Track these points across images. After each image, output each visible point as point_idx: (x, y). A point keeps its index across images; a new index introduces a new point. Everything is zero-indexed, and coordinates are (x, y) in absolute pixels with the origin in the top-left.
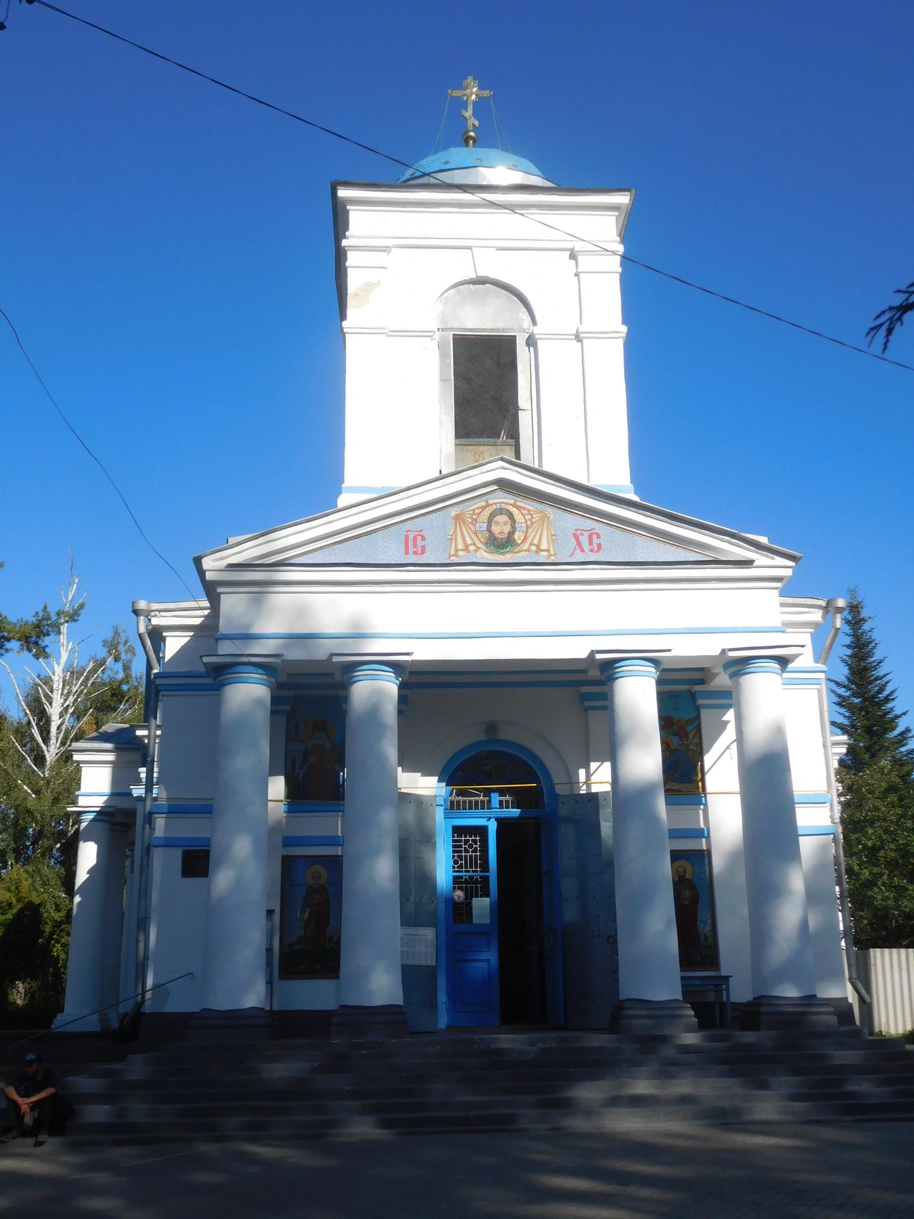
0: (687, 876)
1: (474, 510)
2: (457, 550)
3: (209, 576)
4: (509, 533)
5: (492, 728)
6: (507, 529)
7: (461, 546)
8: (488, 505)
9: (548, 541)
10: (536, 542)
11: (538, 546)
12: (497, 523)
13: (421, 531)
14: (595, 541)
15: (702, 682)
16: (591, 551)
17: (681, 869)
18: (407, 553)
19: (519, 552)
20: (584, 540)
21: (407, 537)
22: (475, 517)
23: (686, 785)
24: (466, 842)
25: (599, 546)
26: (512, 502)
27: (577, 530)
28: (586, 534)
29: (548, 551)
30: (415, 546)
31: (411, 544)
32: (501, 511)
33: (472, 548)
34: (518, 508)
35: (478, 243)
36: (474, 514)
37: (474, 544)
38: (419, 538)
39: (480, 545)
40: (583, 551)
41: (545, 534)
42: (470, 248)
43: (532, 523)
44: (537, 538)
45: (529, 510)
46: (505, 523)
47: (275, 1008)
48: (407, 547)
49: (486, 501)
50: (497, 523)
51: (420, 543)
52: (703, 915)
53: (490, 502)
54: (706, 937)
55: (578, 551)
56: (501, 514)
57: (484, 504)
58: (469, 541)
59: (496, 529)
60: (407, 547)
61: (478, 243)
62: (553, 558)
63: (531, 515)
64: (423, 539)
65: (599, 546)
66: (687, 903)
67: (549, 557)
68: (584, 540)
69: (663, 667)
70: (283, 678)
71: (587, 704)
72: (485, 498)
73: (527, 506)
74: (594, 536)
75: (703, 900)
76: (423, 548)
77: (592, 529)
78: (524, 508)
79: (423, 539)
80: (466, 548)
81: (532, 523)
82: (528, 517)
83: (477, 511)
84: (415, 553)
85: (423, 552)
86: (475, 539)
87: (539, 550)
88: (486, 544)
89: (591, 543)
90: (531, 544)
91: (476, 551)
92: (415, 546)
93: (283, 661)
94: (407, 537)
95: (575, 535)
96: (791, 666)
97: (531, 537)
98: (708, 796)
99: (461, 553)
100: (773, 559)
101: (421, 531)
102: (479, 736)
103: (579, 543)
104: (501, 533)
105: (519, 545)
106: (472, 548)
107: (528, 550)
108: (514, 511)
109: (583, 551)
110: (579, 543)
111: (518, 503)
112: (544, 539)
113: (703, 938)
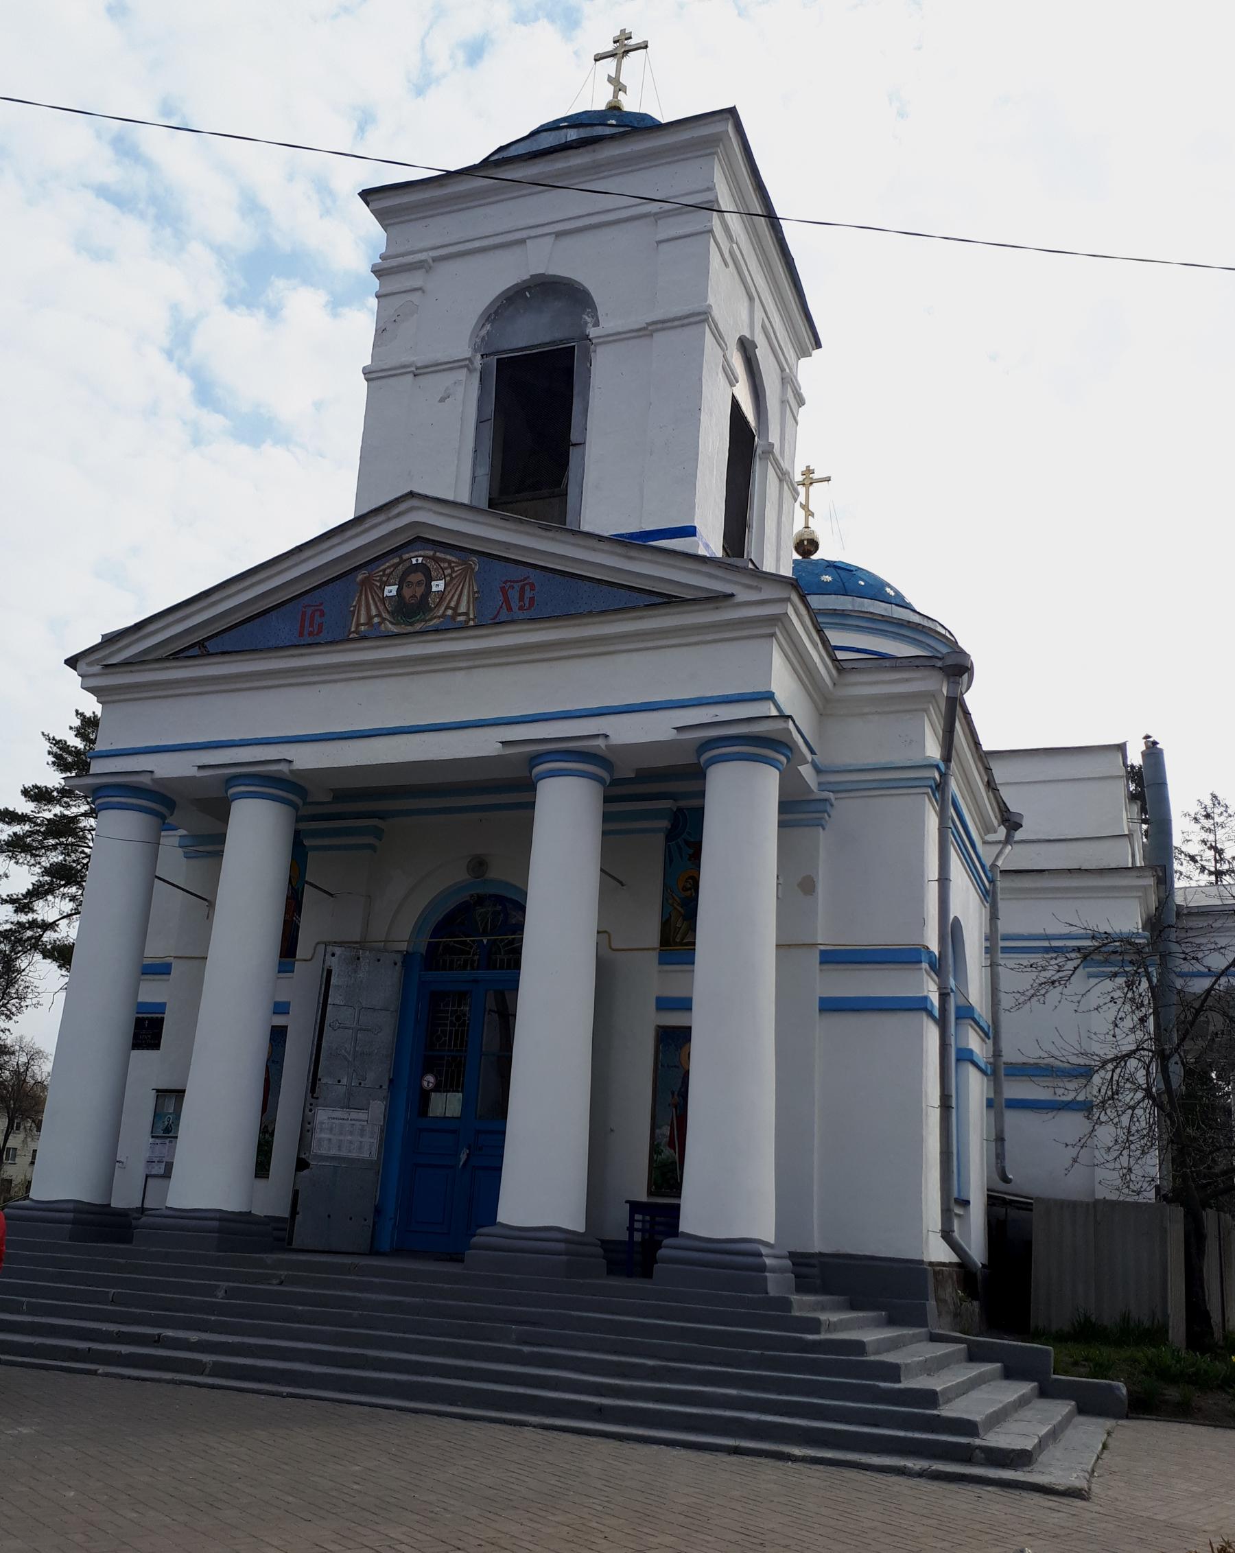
1: (384, 570)
2: (358, 625)
5: (479, 865)
6: (420, 591)
8: (402, 561)
9: (468, 602)
10: (453, 604)
11: (455, 609)
14: (528, 594)
16: (521, 608)
18: (301, 634)
19: (431, 620)
20: (514, 595)
21: (304, 614)
22: (384, 579)
25: (532, 600)
26: (431, 553)
27: (505, 582)
28: (517, 586)
29: (467, 614)
30: (311, 625)
31: (307, 624)
33: (376, 620)
34: (436, 560)
35: (533, 233)
37: (379, 615)
38: (318, 614)
39: (385, 615)
40: (510, 609)
41: (466, 591)
42: (522, 242)
43: (452, 579)
45: (450, 562)
46: (419, 583)
48: (302, 627)
49: (400, 557)
50: (410, 584)
51: (317, 619)
53: (406, 556)
55: (505, 610)
56: (415, 572)
57: (396, 560)
58: (374, 612)
59: (407, 592)
60: (302, 627)
61: (533, 233)
63: (452, 568)
65: (532, 600)
67: (467, 622)
68: (514, 595)
72: (399, 553)
73: (448, 557)
74: (527, 588)
76: (321, 625)
78: (444, 560)
79: (322, 614)
81: (452, 579)
83: (388, 571)
84: (310, 634)
85: (320, 631)
86: (381, 608)
87: (456, 613)
88: (391, 613)
89: (521, 599)
90: (448, 607)
92: (311, 625)
93: (155, 781)
94: (304, 614)
95: (503, 589)
99: (363, 628)
102: (458, 874)
103: (507, 600)
105: (431, 610)
107: (443, 616)
108: (431, 565)
109: (510, 609)
110: (507, 600)
111: (438, 554)
112: (465, 598)
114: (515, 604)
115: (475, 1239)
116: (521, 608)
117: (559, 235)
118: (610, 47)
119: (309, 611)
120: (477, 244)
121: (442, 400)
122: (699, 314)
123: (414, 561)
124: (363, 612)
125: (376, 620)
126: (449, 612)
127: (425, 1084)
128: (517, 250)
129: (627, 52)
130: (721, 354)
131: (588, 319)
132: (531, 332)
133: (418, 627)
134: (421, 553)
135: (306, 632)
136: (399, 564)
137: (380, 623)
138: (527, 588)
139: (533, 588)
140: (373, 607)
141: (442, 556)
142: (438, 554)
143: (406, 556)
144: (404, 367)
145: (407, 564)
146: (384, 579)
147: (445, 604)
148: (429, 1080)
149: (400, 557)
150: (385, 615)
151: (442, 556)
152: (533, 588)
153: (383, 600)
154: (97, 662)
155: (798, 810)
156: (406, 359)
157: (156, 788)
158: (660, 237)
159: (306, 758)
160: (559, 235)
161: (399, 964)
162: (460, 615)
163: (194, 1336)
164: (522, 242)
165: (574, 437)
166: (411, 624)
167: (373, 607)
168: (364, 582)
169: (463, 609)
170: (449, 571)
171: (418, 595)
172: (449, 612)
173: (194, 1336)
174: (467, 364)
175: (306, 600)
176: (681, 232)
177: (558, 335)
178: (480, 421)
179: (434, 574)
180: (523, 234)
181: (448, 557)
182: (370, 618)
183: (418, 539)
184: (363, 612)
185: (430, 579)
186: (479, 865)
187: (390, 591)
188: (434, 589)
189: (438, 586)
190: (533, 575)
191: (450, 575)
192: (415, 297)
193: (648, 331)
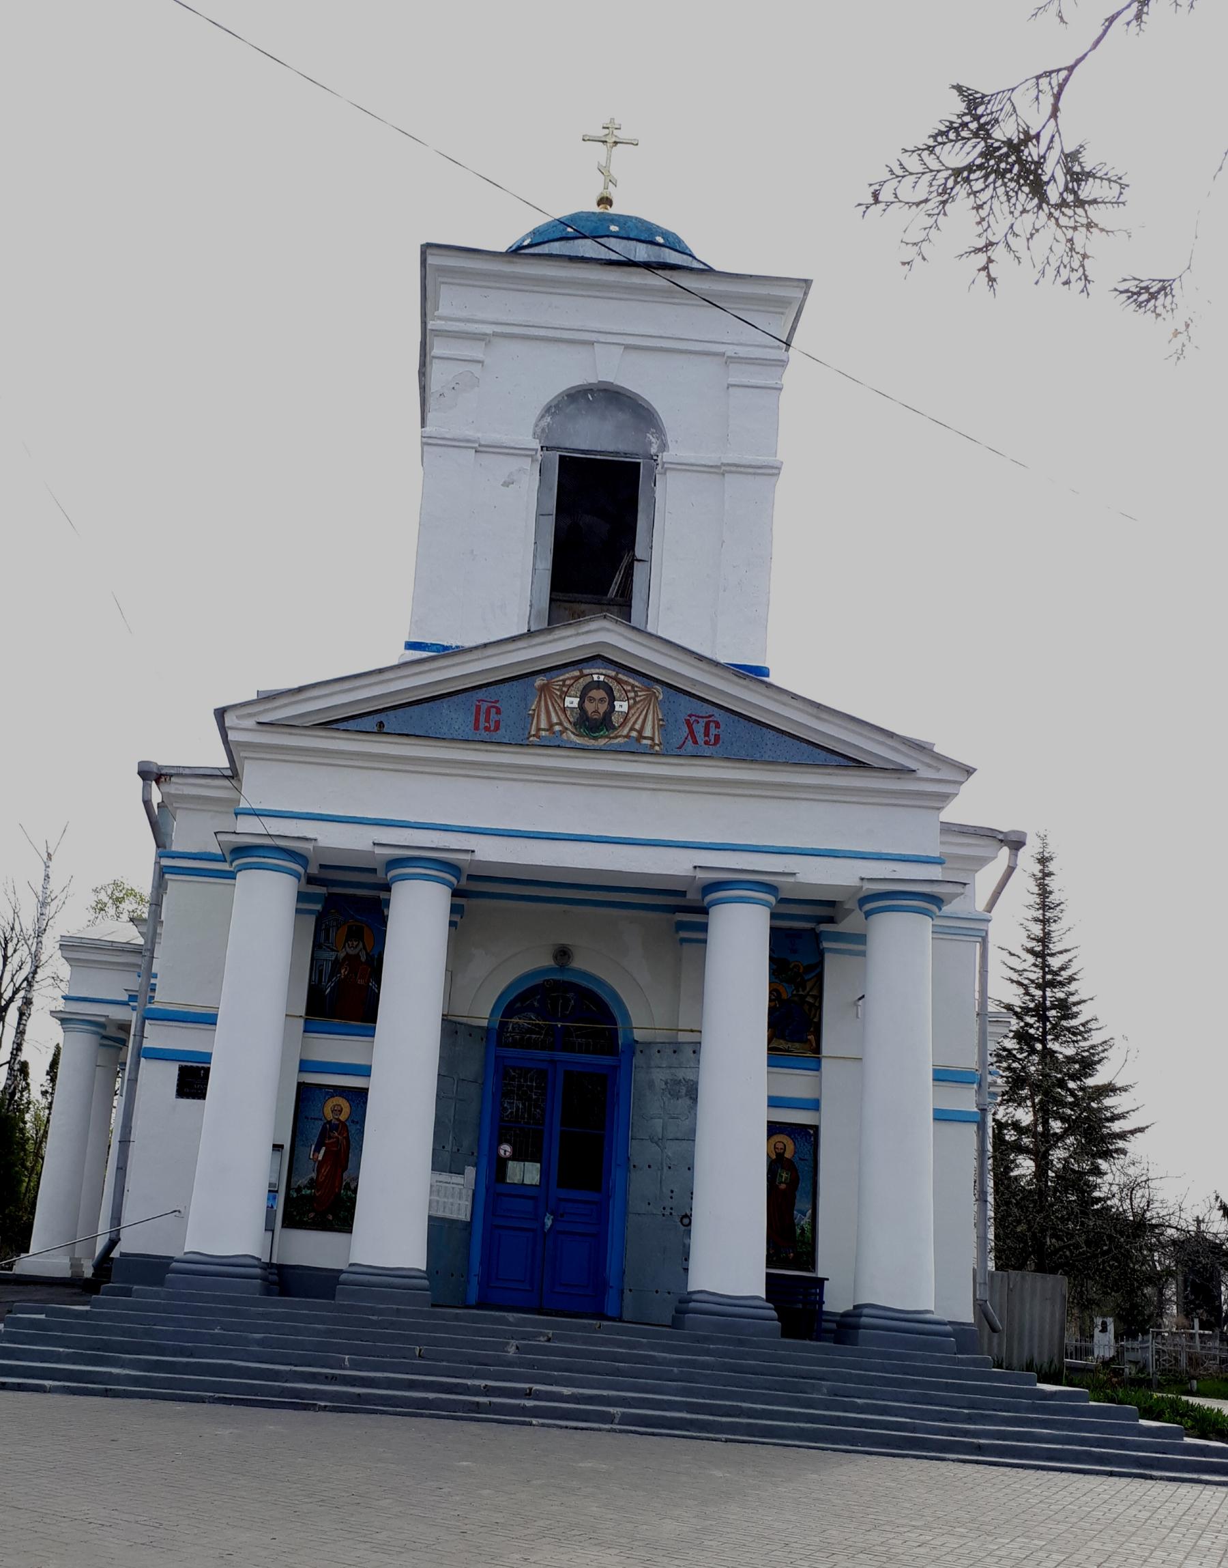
0: (788, 1155)
1: (564, 681)
2: (539, 729)
3: (232, 736)
4: (605, 713)
5: (563, 954)
6: (603, 708)
7: (543, 725)
10: (637, 727)
11: (640, 732)
12: (592, 699)
13: (497, 701)
14: (713, 731)
15: (831, 920)
16: (706, 743)
17: (780, 1146)
18: (477, 728)
20: (699, 729)
21: (478, 708)
22: (565, 689)
23: (797, 1045)
25: (717, 737)
26: (613, 674)
27: (690, 716)
28: (702, 722)
30: (487, 720)
31: (482, 718)
32: (598, 685)
34: (619, 682)
35: (602, 338)
36: (564, 685)
37: (560, 724)
39: (567, 725)
40: (695, 742)
41: (650, 717)
42: (592, 343)
43: (636, 703)
45: (633, 686)
46: (601, 700)
47: (274, 1261)
48: (477, 720)
49: (581, 671)
50: (592, 699)
52: (802, 1204)
53: (586, 671)
54: (803, 1229)
55: (690, 742)
57: (577, 673)
58: (555, 720)
59: (590, 707)
60: (477, 720)
61: (602, 338)
62: (657, 748)
63: (636, 692)
64: (498, 712)
65: (717, 737)
66: (783, 1186)
67: (652, 746)
68: (699, 729)
69: (782, 895)
70: (313, 870)
71: (683, 934)
72: (580, 666)
73: (631, 681)
74: (712, 725)
75: (804, 1185)
76: (497, 724)
78: (627, 683)
79: (498, 712)
80: (551, 725)
81: (636, 703)
82: (631, 695)
83: (568, 682)
85: (497, 728)
86: (562, 717)
87: (641, 736)
88: (575, 724)
89: (707, 734)
90: (632, 729)
91: (561, 732)
94: (478, 708)
95: (688, 723)
96: (946, 909)
97: (633, 720)
98: (824, 1062)
99: (543, 733)
101: (497, 701)
102: (547, 961)
103: (692, 732)
104: (596, 711)
105: (614, 728)
106: (557, 728)
107: (627, 736)
108: (613, 685)
109: (695, 742)
110: (692, 732)
111: (620, 676)
113: (799, 1231)
114: (701, 738)
116: (706, 743)
117: (627, 347)
118: (601, 133)
119: (484, 706)
120: (542, 332)
121: (506, 484)
122: (772, 467)
123: (595, 677)
125: (557, 728)
126: (634, 734)
127: (502, 1152)
129: (616, 143)
131: (653, 440)
132: (596, 436)
133: (602, 742)
134: (604, 671)
135: (481, 727)
136: (577, 679)
137: (561, 732)
138: (712, 725)
139: (718, 726)
140: (553, 714)
141: (625, 678)
143: (586, 671)
144: (468, 441)
145: (588, 679)
146: (565, 689)
147: (629, 725)
148: (506, 1150)
150: (567, 725)
151: (625, 678)
153: (564, 710)
154: (250, 715)
156: (470, 433)
158: (732, 380)
162: (645, 738)
163: (566, 1391)
165: (639, 552)
166: (595, 738)
167: (553, 714)
168: (543, 688)
169: (647, 733)
171: (602, 711)
172: (634, 734)
173: (566, 1391)
175: (481, 694)
176: (745, 381)
177: (621, 447)
178: (540, 515)
179: (616, 694)
180: (593, 337)
181: (631, 681)
182: (551, 725)
183: (599, 657)
186: (563, 954)
187: (572, 702)
189: (621, 706)
190: (718, 715)
192: (476, 369)
193: (720, 470)
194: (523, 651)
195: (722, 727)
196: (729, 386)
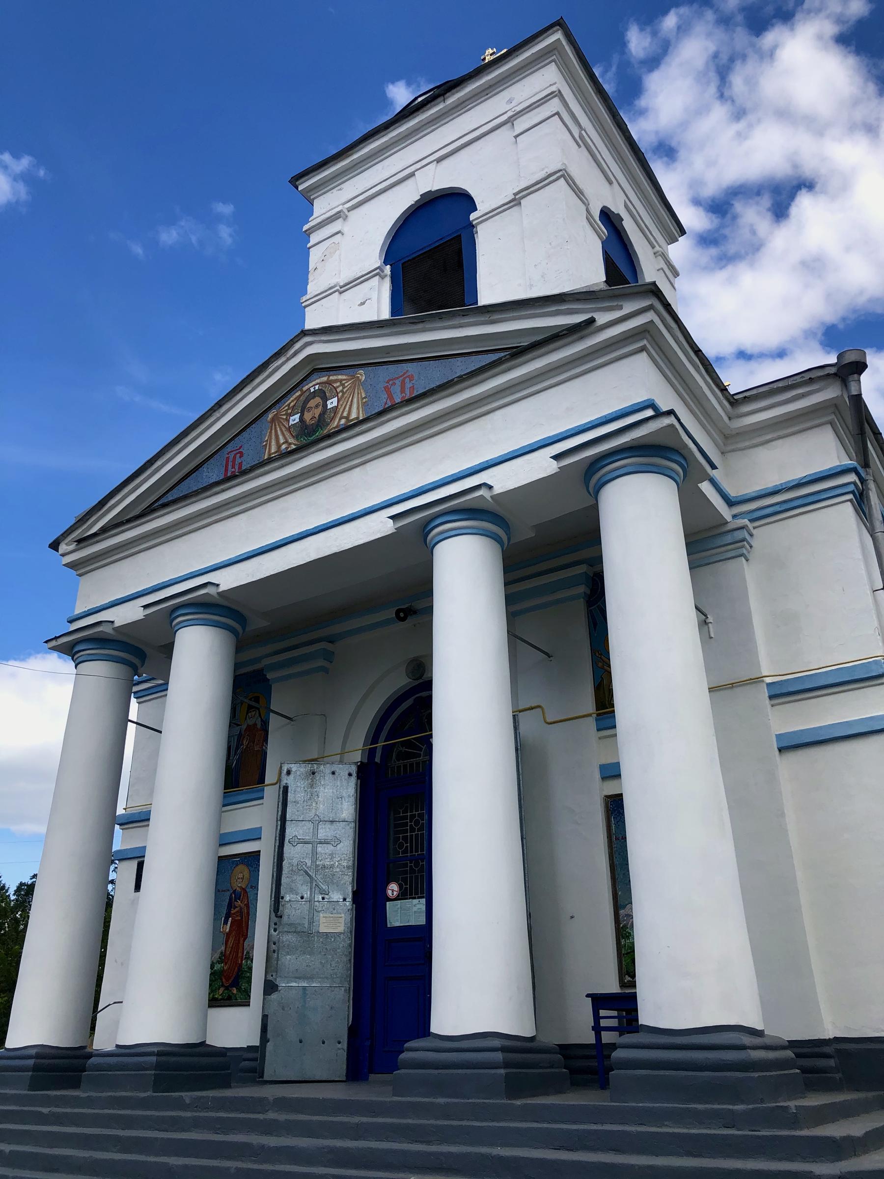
9: (358, 408)
10: (345, 414)
22: (289, 411)
24: (413, 817)
26: (325, 379)
28: (398, 382)
30: (233, 467)
41: (355, 400)
42: (412, 175)
43: (344, 393)
44: (347, 409)
45: (341, 381)
46: (317, 406)
49: (301, 390)
53: (305, 389)
58: (282, 441)
59: (308, 416)
72: (300, 387)
73: (340, 377)
74: (407, 380)
77: (405, 374)
78: (336, 381)
81: (344, 393)
83: (292, 404)
86: (287, 434)
92: (233, 467)
94: (228, 458)
100: (620, 308)
111: (331, 378)
115: (402, 1056)
119: (232, 456)
123: (312, 390)
124: (273, 443)
128: (410, 181)
130: (584, 208)
138: (407, 380)
140: (281, 437)
142: (331, 378)
143: (305, 389)
145: (307, 394)
146: (289, 411)
147: (339, 415)
149: (301, 390)
152: (411, 378)
155: (708, 542)
157: (120, 638)
158: (517, 132)
159: (228, 580)
160: (439, 160)
161: (355, 774)
164: (412, 175)
167: (281, 437)
168: (273, 420)
170: (341, 388)
171: (317, 416)
174: (376, 273)
175: (229, 448)
181: (340, 377)
184: (273, 443)
185: (325, 399)
188: (329, 406)
191: (342, 391)
193: (516, 201)
194: (250, 395)
195: (416, 377)
196: (516, 137)
